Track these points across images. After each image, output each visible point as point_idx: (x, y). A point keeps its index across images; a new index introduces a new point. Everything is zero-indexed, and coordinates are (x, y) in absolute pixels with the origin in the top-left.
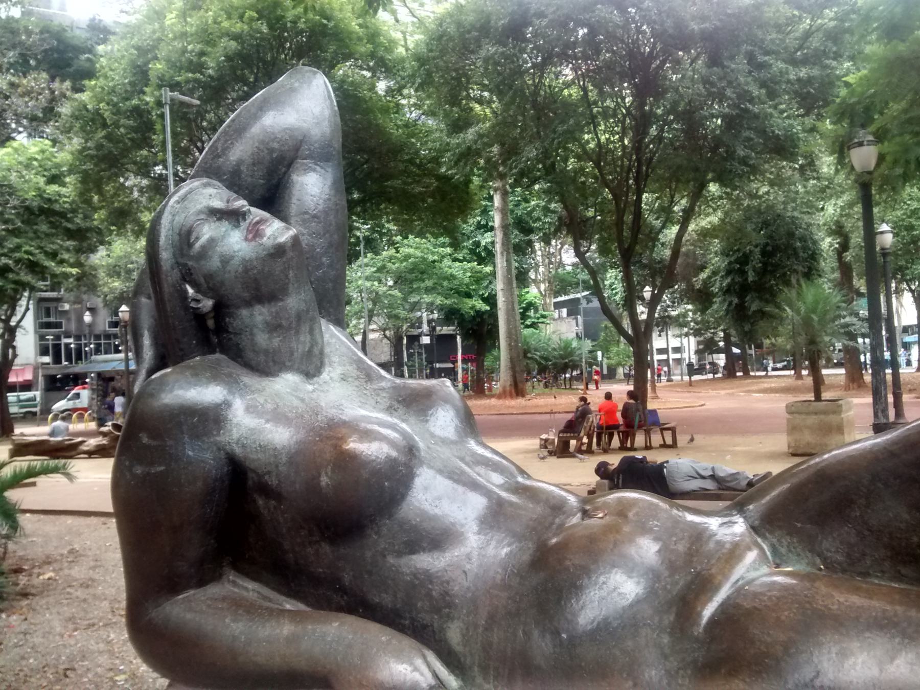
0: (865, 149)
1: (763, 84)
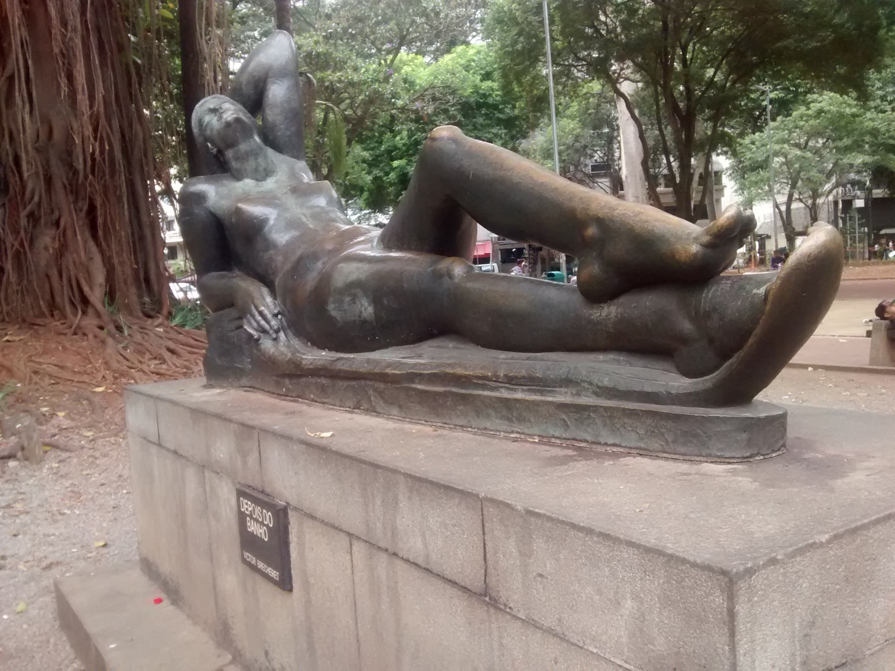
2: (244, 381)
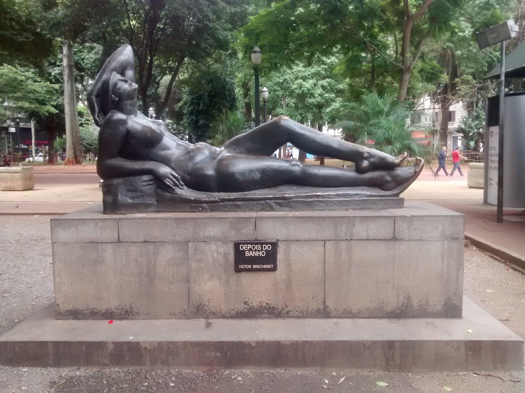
0: (257, 54)
1: (215, 12)
2: (151, 209)
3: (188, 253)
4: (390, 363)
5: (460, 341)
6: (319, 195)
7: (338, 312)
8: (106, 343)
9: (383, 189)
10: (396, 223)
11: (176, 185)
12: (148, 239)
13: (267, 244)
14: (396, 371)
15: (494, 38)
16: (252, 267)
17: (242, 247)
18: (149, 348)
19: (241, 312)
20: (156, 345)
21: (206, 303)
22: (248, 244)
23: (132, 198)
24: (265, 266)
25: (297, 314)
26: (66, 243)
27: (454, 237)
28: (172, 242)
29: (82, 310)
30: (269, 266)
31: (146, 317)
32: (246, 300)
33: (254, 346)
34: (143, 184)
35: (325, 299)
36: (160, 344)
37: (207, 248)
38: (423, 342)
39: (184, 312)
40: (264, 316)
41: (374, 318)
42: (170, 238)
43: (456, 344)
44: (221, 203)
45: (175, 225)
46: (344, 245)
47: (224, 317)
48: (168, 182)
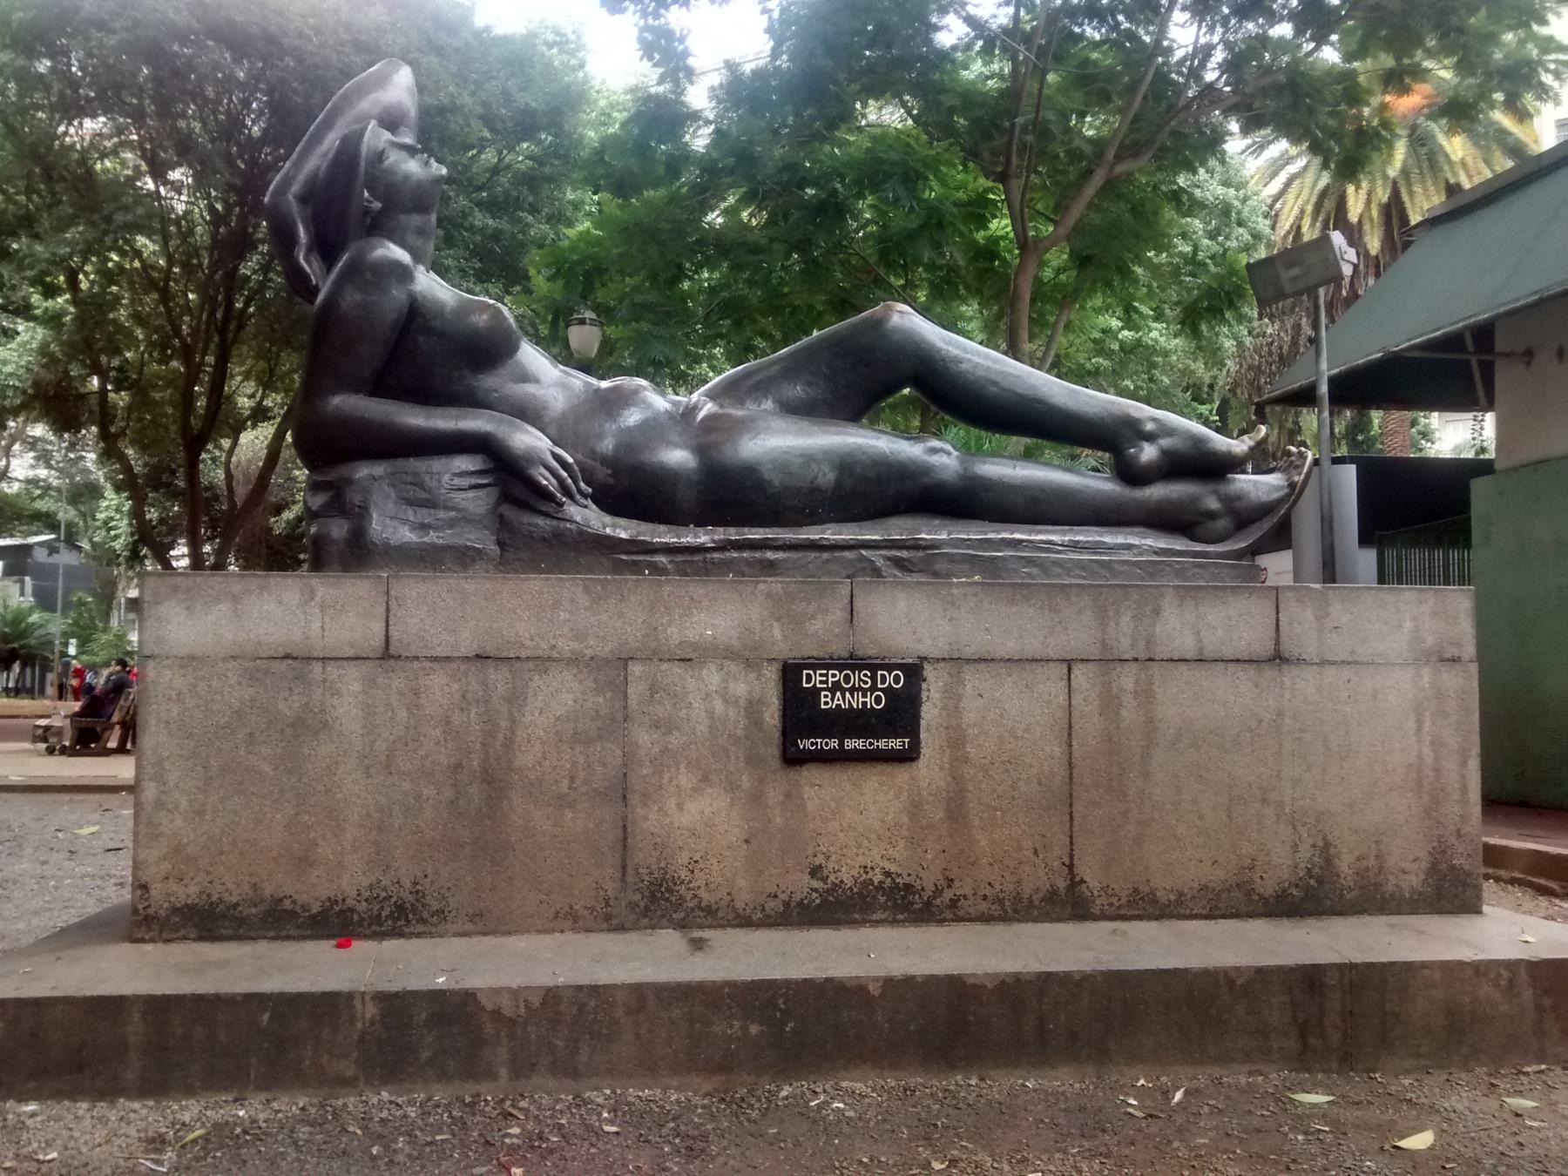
0: (586, 328)
3: (626, 696)
4: (1312, 1041)
5: (1519, 962)
6: (1021, 541)
7: (1114, 900)
8: (350, 996)
9: (1194, 539)
10: (1282, 607)
11: (566, 492)
12: (490, 650)
13: (890, 668)
14: (1330, 1070)
15: (1295, 279)
16: (841, 744)
17: (809, 676)
18: (507, 1012)
19: (800, 904)
20: (536, 1001)
21: (683, 874)
22: (828, 667)
23: (423, 527)
24: (881, 744)
25: (983, 907)
26: (193, 658)
27: (1448, 655)
28: (574, 661)
29: (236, 905)
30: (895, 744)
31: (469, 927)
32: (819, 860)
33: (876, 993)
34: (457, 481)
35: (1071, 856)
36: (552, 995)
37: (691, 685)
38: (1409, 967)
39: (607, 904)
40: (874, 917)
41: (1224, 917)
42: (566, 646)
43: (1505, 974)
44: (716, 555)
45: (584, 601)
46: (1127, 678)
47: (744, 921)
48: (546, 480)
